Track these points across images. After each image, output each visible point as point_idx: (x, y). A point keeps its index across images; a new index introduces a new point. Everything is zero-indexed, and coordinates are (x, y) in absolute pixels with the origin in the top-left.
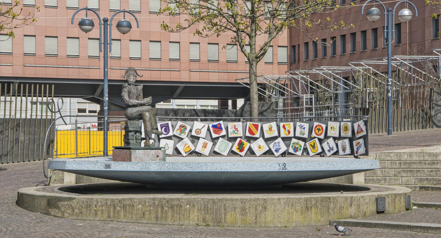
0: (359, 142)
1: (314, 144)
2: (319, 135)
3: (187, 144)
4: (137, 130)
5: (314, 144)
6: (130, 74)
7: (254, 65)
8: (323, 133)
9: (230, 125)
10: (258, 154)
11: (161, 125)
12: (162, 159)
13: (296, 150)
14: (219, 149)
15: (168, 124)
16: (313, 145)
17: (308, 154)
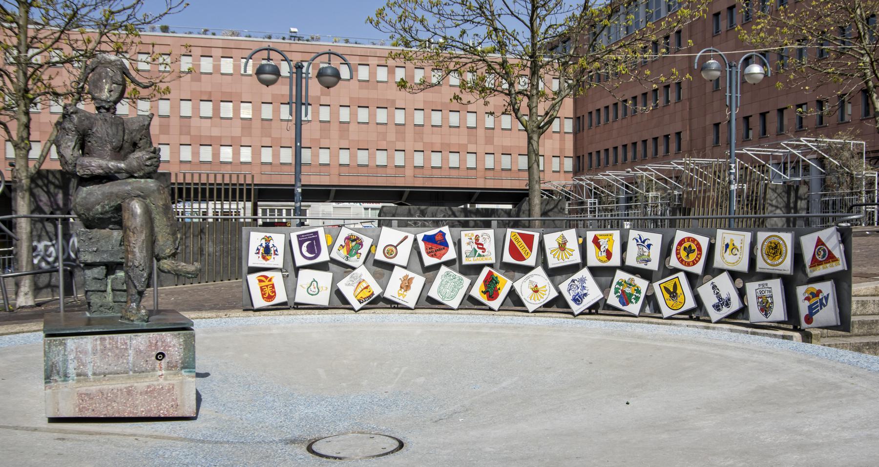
0: (820, 291)
1: (675, 286)
2: (688, 264)
3: (364, 280)
4: (111, 260)
5: (675, 286)
6: (100, 74)
7: (534, 138)
8: (699, 259)
9: (466, 235)
10: (531, 307)
11: (299, 236)
13: (625, 299)
14: (439, 292)
16: (672, 290)
17: (657, 309)
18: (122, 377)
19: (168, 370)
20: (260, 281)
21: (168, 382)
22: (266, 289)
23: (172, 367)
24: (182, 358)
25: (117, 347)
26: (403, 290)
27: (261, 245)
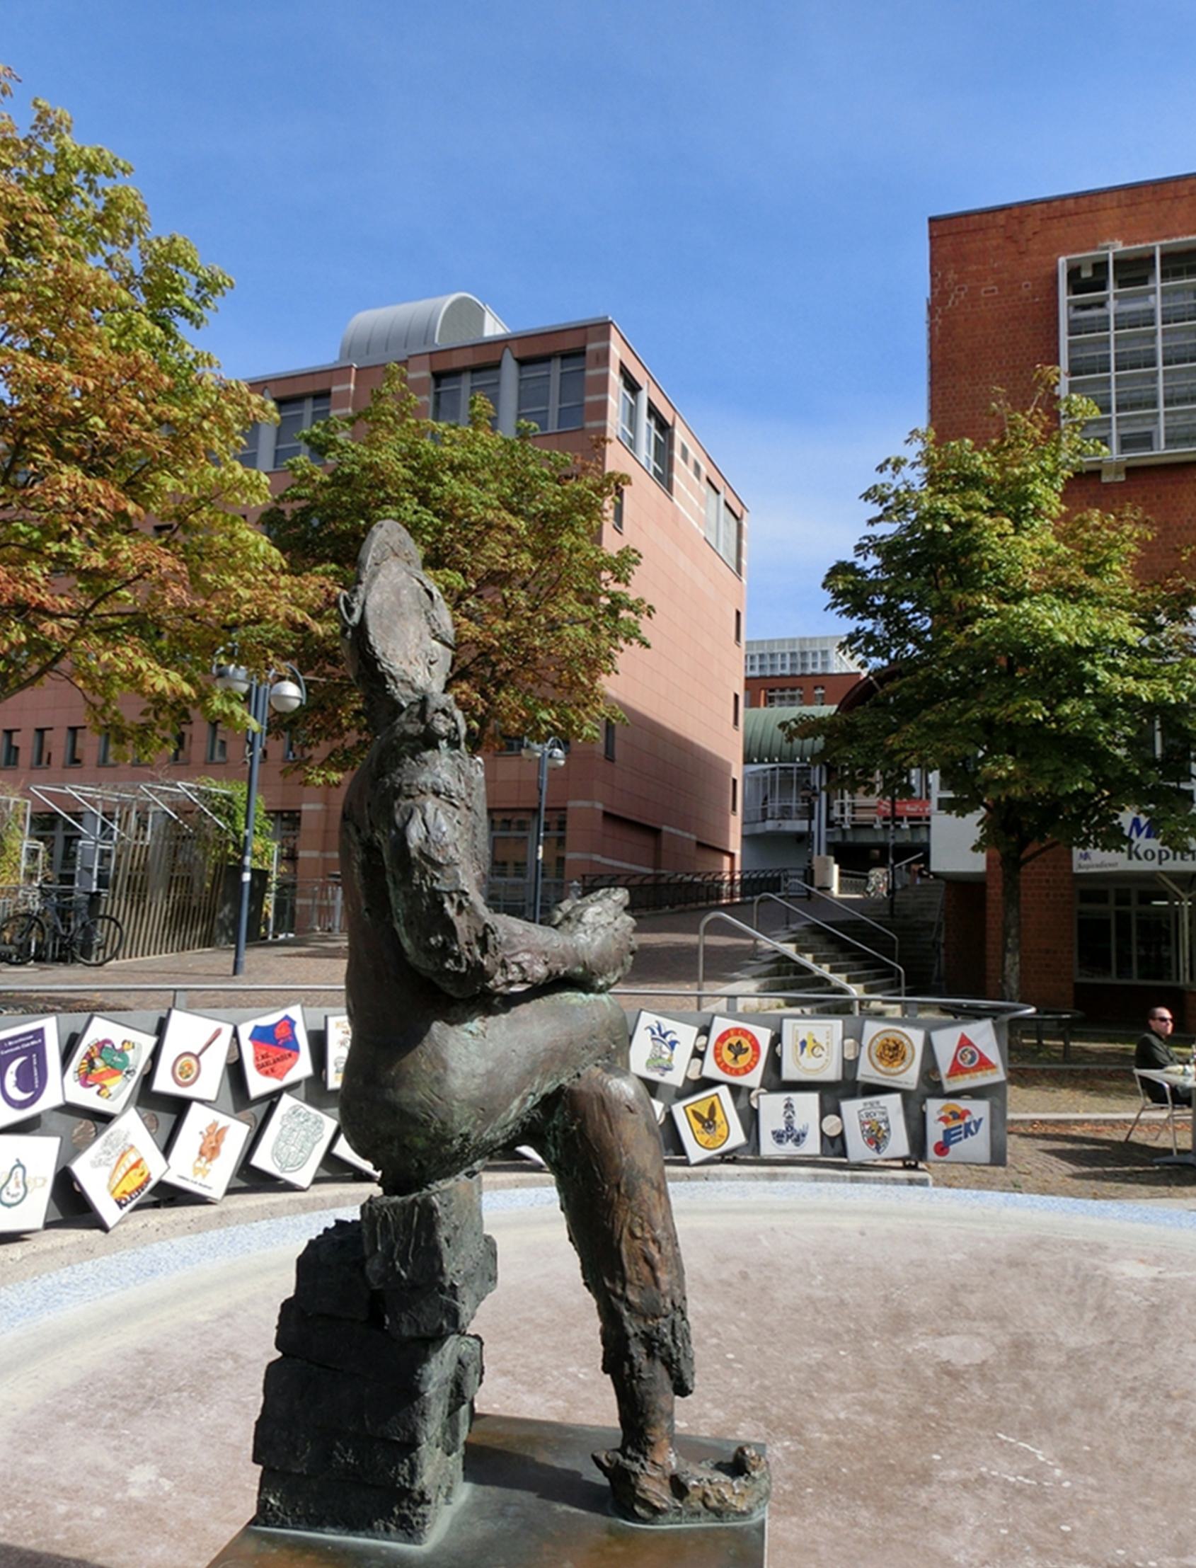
0: (967, 1112)
1: (712, 1110)
2: (736, 1073)
3: (132, 1147)
5: (712, 1110)
8: (756, 1063)
14: (275, 1154)
15: (39, 1033)
16: (706, 1116)
17: (681, 1149)
26: (204, 1159)
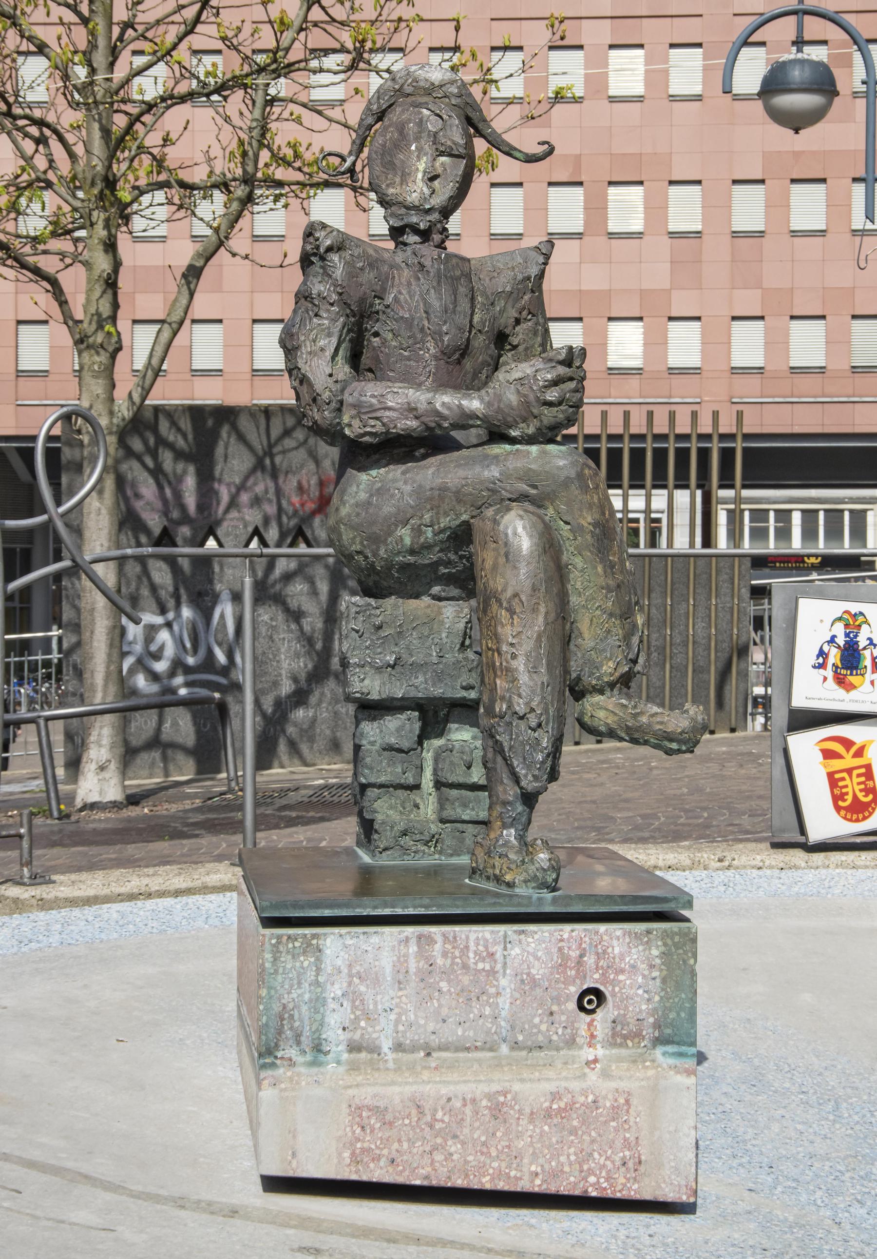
4: (438, 691)
12: (648, 1032)
18: (479, 1061)
19: (614, 1045)
20: (828, 754)
21: (613, 1085)
22: (848, 782)
23: (625, 1037)
24: (655, 1010)
25: (465, 966)
27: (832, 640)
